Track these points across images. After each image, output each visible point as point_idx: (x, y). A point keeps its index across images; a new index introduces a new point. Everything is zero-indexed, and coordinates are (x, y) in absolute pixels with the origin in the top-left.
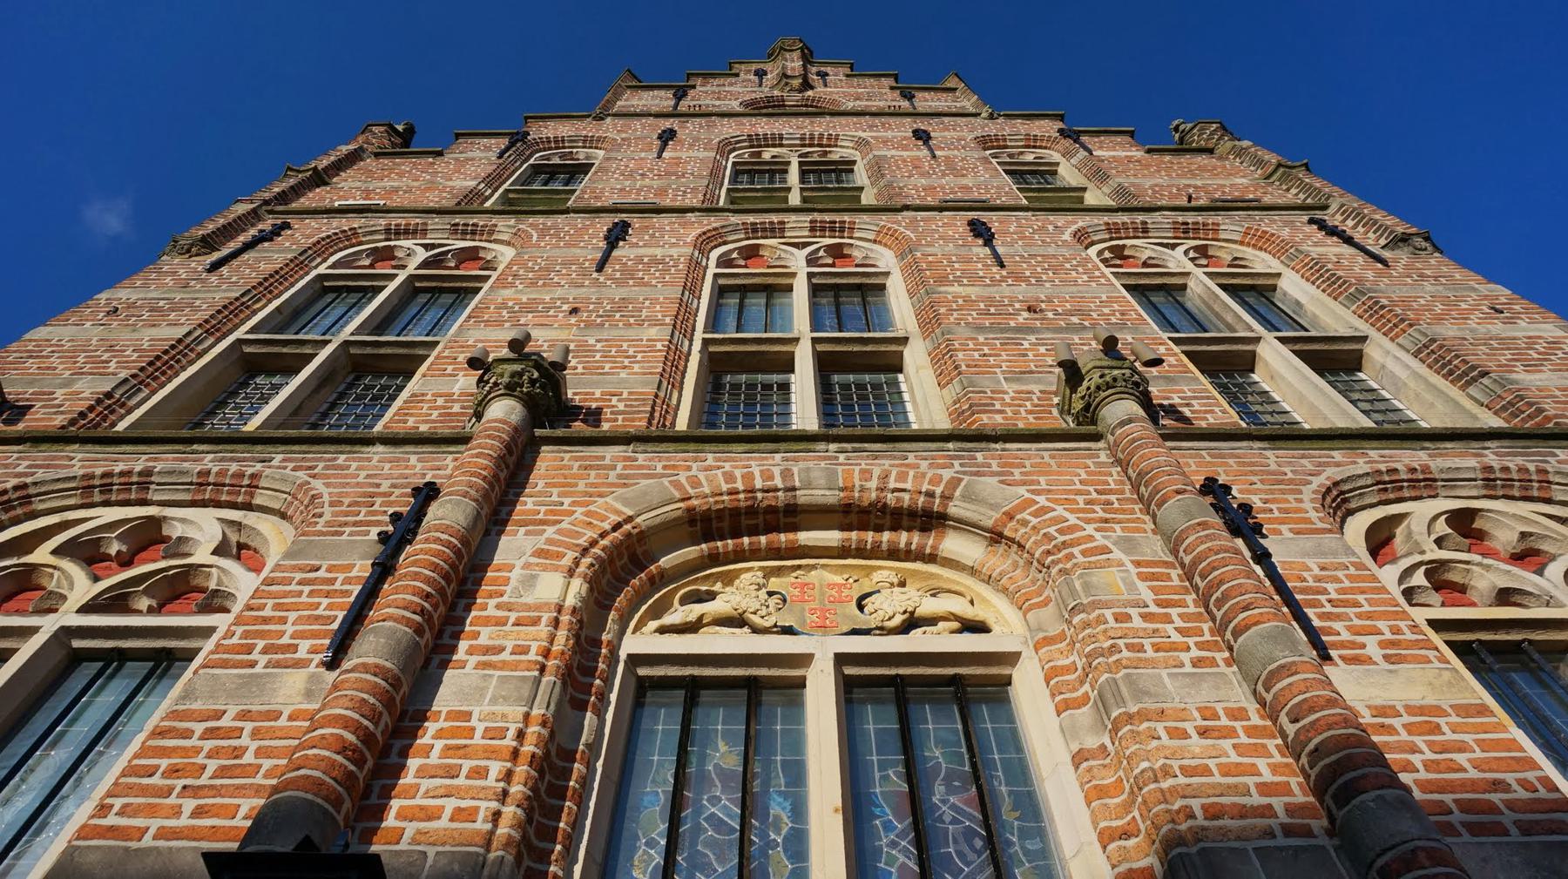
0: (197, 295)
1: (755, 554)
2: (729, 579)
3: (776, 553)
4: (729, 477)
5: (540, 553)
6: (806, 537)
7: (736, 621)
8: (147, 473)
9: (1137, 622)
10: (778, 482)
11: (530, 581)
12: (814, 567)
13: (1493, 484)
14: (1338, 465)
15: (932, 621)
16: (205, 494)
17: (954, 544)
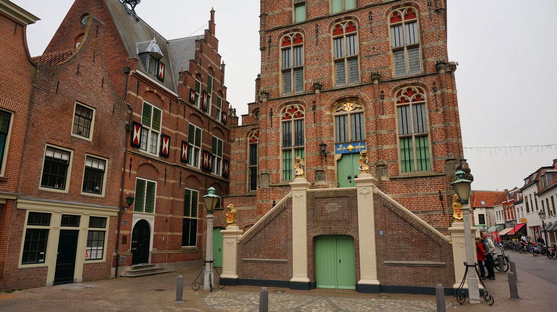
0: (272, 63)
1: (342, 102)
2: (341, 104)
3: (344, 101)
4: (339, 95)
5: (325, 109)
6: (346, 100)
7: (342, 110)
8: (289, 102)
9: (371, 112)
10: (343, 96)
11: (325, 112)
12: (347, 103)
13: (413, 84)
14: (397, 84)
15: (357, 108)
16: (295, 102)
17: (359, 100)
